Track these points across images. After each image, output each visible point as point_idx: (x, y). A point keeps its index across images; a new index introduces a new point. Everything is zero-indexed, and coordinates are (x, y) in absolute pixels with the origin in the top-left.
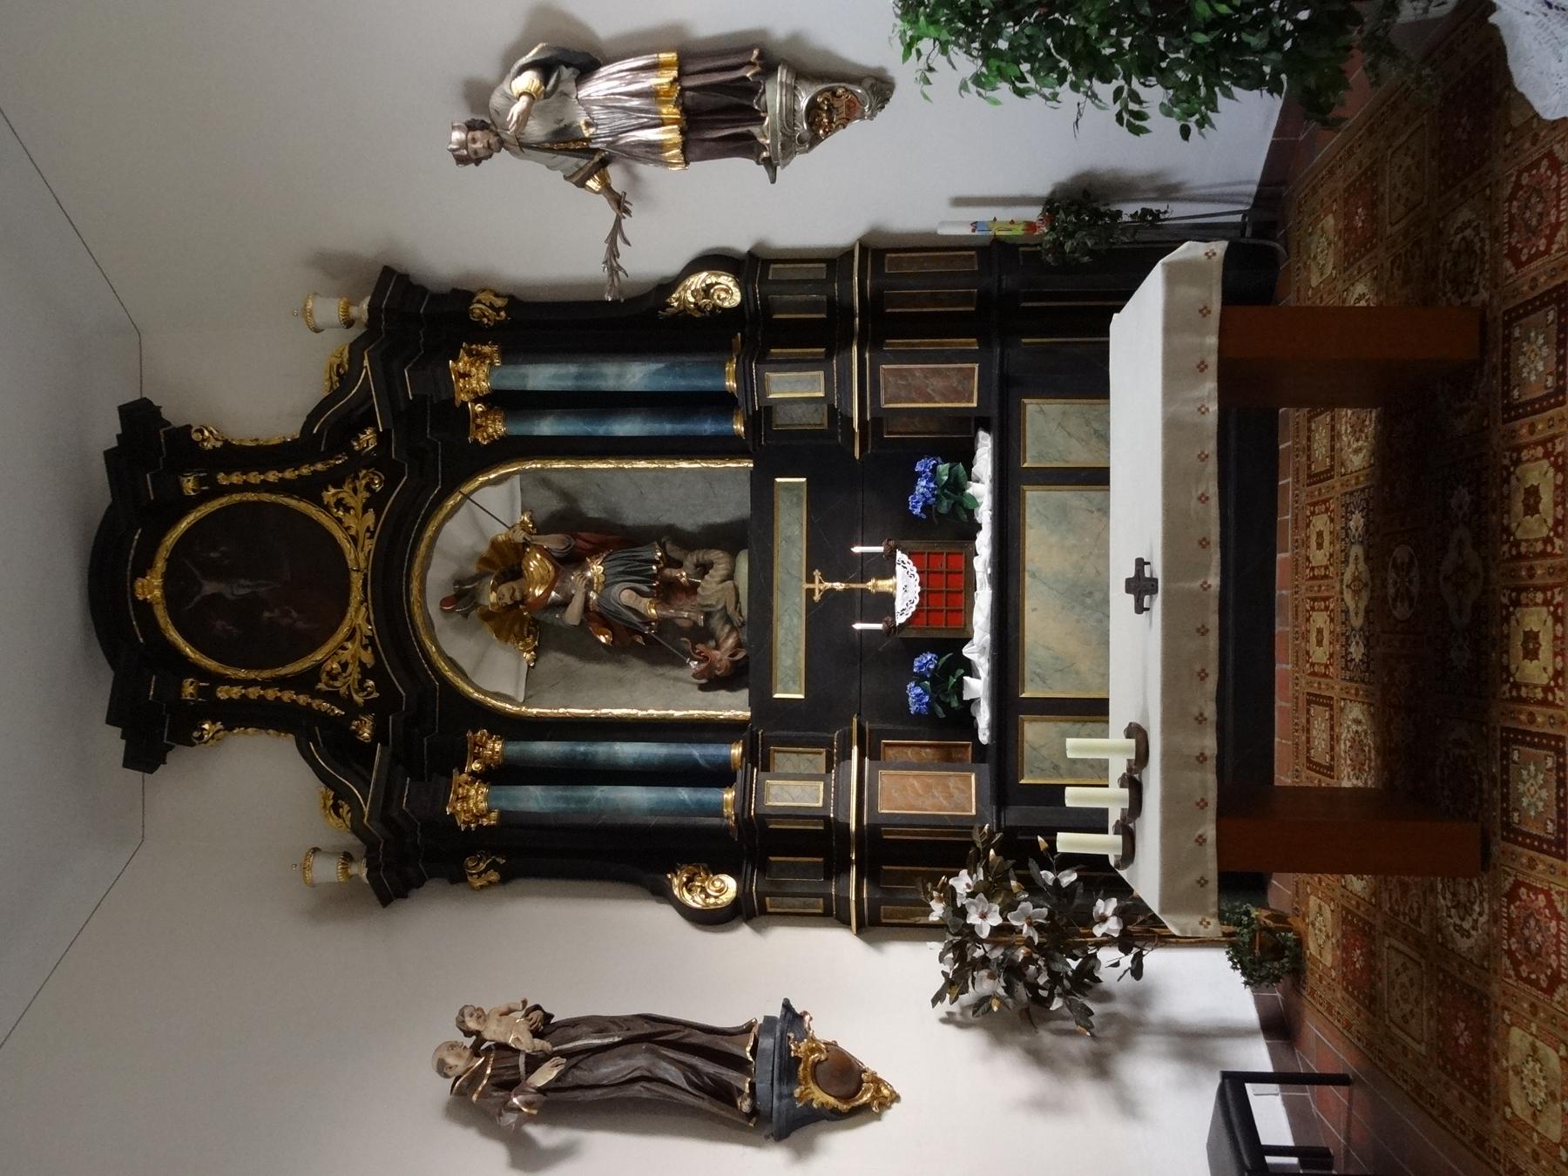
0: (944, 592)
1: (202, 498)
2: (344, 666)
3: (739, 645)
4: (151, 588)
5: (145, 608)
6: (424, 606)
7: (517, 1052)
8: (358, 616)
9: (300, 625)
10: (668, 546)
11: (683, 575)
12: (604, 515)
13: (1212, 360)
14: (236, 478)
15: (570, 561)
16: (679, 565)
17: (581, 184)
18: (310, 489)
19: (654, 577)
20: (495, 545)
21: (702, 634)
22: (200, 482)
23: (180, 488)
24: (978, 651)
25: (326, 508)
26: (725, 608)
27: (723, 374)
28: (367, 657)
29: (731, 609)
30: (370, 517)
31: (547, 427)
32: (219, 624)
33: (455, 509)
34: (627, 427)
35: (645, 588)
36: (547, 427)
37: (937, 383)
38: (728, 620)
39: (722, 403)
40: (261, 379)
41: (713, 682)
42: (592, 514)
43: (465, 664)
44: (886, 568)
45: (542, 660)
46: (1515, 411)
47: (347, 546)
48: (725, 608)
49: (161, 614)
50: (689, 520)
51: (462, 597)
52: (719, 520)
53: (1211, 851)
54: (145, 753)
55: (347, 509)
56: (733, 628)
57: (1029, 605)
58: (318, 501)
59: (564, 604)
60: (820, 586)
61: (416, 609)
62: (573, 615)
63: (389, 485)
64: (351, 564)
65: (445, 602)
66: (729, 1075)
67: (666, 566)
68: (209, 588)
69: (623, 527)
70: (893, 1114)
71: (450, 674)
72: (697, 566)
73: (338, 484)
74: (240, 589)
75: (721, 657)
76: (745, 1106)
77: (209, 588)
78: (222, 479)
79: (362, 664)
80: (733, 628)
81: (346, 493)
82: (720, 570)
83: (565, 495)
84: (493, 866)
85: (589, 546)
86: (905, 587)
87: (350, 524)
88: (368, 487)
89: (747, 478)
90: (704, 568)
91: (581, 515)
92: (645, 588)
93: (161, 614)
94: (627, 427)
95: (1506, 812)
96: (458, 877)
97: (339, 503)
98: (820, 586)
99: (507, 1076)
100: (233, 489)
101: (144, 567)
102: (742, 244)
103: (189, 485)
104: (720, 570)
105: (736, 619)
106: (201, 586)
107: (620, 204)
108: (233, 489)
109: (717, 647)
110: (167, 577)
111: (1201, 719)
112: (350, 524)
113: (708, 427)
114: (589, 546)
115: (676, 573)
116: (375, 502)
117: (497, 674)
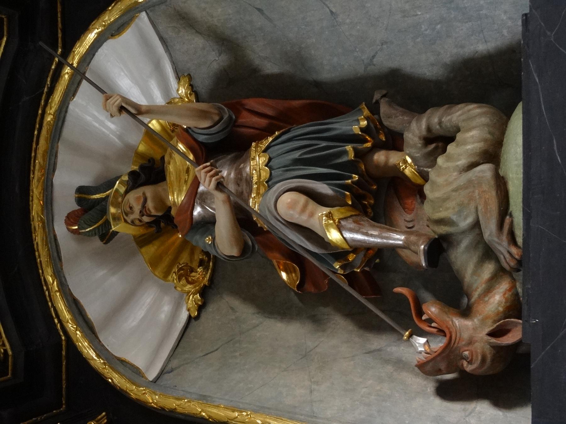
3: (514, 309)
10: (384, 109)
11: (407, 163)
12: (287, 68)
16: (395, 142)
19: (351, 167)
26: (477, 225)
29: (490, 229)
35: (323, 188)
38: (488, 253)
42: (271, 68)
43: (93, 311)
45: (211, 308)
48: (477, 225)
50: (425, 61)
56: (501, 272)
65: (71, 219)
67: (378, 146)
69: (318, 84)
71: (71, 326)
72: (427, 140)
80: (501, 272)
83: (225, 41)
85: (263, 122)
91: (254, 71)
92: (323, 188)
109: (466, 312)
114: (263, 122)
115: (394, 158)
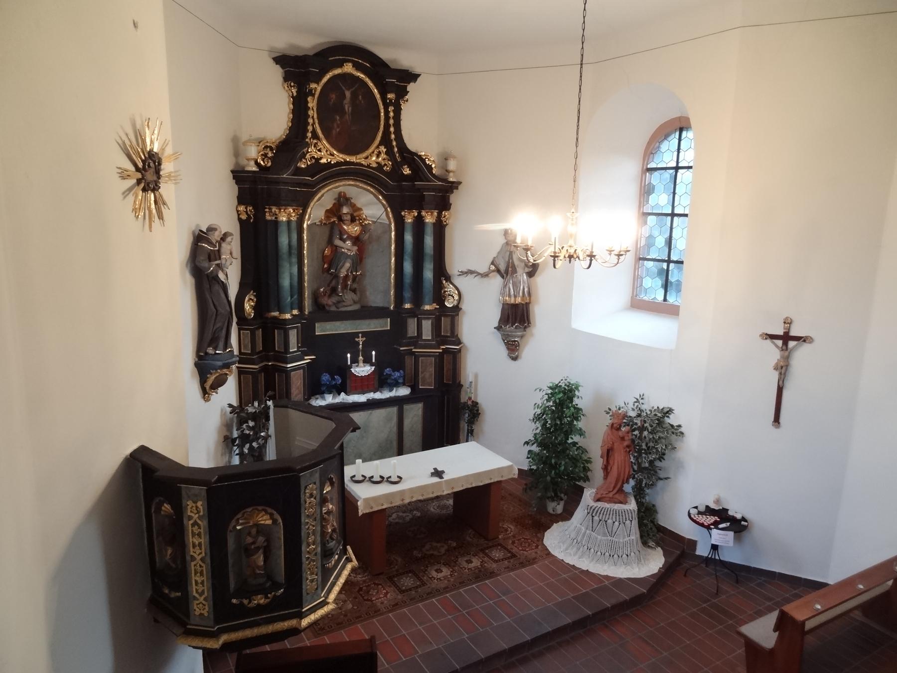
0: (363, 385)
1: (384, 98)
2: (320, 150)
4: (348, 68)
5: (340, 64)
6: (344, 185)
7: (220, 259)
8: (340, 157)
9: (334, 132)
13: (492, 481)
14: (392, 114)
15: (356, 240)
17: (492, 263)
18: (386, 141)
20: (360, 209)
21: (334, 291)
22: (391, 101)
23: (389, 92)
24: (343, 398)
25: (378, 147)
27: (430, 304)
28: (324, 161)
30: (374, 165)
31: (408, 238)
32: (334, 96)
33: (378, 199)
34: (408, 267)
36: (408, 238)
37: (427, 375)
38: (339, 302)
39: (418, 301)
40: (422, 126)
41: (315, 297)
44: (367, 361)
46: (483, 551)
47: (364, 155)
49: (338, 71)
51: (342, 200)
52: (368, 293)
53: (380, 508)
54: (282, 60)
55: (378, 156)
57: (361, 413)
58: (380, 144)
59: (341, 239)
60: (361, 340)
61: (341, 184)
62: (338, 242)
63: (386, 173)
64: (358, 157)
66: (221, 344)
68: (348, 94)
70: (202, 401)
73: (386, 153)
74: (347, 108)
75: (325, 301)
76: (210, 351)
77: (348, 94)
78: (391, 109)
79: (321, 158)
81: (383, 156)
82: (355, 297)
84: (249, 217)
86: (362, 370)
87: (374, 157)
88: (385, 165)
89: (386, 305)
90: (354, 291)
93: (338, 71)
94: (408, 267)
95: (397, 575)
96: (241, 200)
97: (380, 153)
98: (361, 340)
99: (212, 257)
100: (387, 113)
101: (357, 66)
102: (464, 306)
103: (391, 96)
104: (355, 297)
105: (340, 305)
106: (348, 90)
107: (485, 275)
108: (387, 113)
110: (351, 75)
111: (412, 497)
112: (374, 157)
113: (407, 294)
116: (380, 167)
117: (317, 211)
